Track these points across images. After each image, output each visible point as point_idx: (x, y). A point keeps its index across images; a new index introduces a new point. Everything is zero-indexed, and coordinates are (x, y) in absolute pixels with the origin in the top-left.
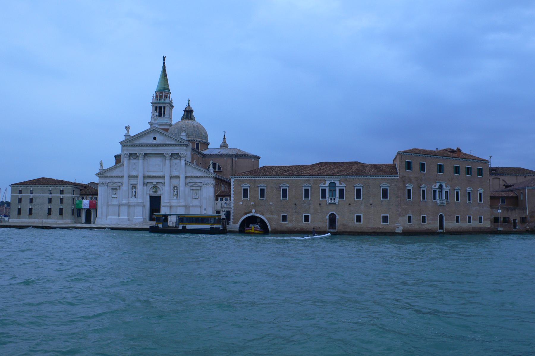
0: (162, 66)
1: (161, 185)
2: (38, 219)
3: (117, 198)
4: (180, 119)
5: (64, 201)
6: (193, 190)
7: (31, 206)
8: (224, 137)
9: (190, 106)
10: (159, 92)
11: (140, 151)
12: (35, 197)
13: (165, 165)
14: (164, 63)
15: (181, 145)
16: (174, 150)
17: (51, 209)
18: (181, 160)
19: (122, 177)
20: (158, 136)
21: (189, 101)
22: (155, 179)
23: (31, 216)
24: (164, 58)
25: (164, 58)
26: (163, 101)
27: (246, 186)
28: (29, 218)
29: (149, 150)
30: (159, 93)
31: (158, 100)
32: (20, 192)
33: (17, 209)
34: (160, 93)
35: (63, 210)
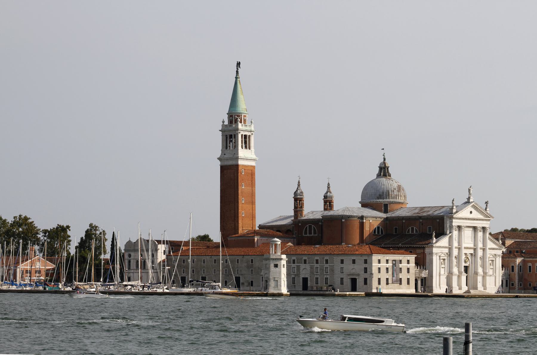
2: (393, 289)
3: (444, 268)
4: (375, 177)
5: (410, 270)
6: (491, 260)
8: (329, 184)
9: (386, 161)
11: (463, 224)
12: (390, 267)
14: (237, 72)
15: (488, 220)
16: (482, 224)
17: (401, 278)
20: (473, 210)
22: (468, 250)
23: (388, 285)
24: (239, 64)
25: (239, 64)
26: (248, 128)
28: (386, 289)
32: (379, 261)
34: (244, 116)
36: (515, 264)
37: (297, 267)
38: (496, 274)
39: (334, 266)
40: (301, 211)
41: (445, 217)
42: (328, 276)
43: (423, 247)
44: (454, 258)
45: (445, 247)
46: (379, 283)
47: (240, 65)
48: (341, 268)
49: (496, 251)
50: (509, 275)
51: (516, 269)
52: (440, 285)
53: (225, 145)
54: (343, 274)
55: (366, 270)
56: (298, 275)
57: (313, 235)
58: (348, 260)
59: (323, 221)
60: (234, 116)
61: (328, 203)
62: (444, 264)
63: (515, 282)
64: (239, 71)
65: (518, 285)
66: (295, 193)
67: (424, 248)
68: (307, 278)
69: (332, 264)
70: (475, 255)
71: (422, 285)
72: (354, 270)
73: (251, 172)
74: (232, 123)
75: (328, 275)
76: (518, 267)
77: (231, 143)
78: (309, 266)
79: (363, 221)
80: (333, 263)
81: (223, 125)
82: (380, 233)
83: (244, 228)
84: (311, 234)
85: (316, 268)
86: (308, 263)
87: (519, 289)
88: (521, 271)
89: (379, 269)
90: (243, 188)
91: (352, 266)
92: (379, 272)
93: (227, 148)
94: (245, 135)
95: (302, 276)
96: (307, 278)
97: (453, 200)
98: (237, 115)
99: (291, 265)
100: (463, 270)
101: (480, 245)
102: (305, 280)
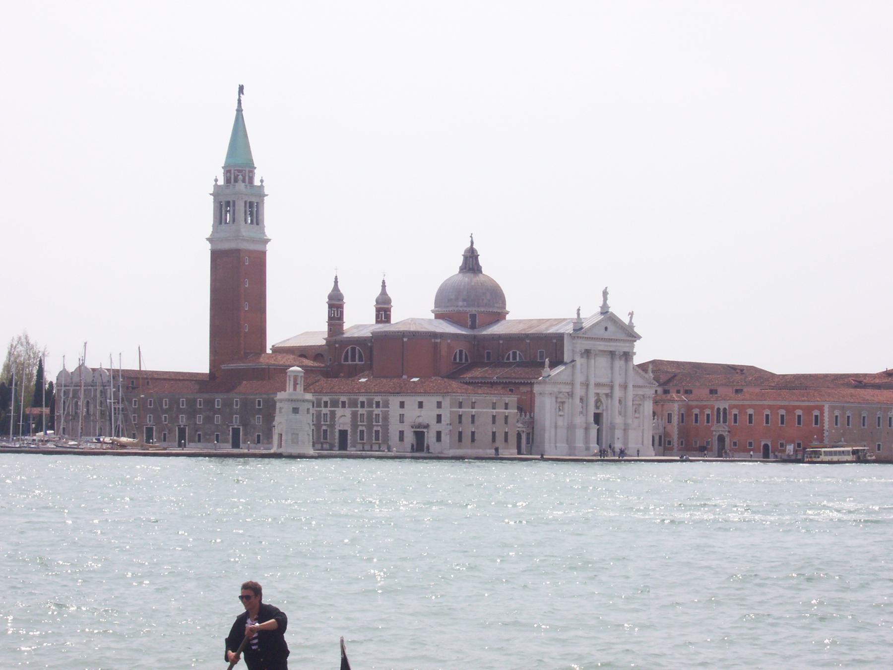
0: (236, 108)
1: (604, 396)
5: (510, 420)
6: (637, 404)
7: (473, 429)
8: (384, 282)
9: (474, 246)
10: (247, 169)
13: (612, 368)
18: (629, 362)
19: (572, 384)
21: (471, 237)
24: (241, 89)
25: (241, 89)
27: (837, 413)
29: (601, 346)
30: (247, 172)
31: (248, 187)
32: (460, 405)
33: (458, 433)
35: (509, 434)
36: (673, 411)
37: (330, 414)
38: (643, 426)
39: (388, 411)
40: (341, 325)
41: (566, 336)
42: (379, 428)
43: (531, 382)
44: (578, 401)
45: (565, 383)
46: (460, 440)
47: (244, 91)
48: (400, 415)
49: (645, 389)
50: (665, 428)
51: (675, 419)
52: (556, 442)
53: (218, 217)
54: (404, 424)
55: (439, 418)
56: (332, 426)
57: (357, 362)
58: (411, 401)
59: (373, 340)
60: (232, 172)
61: (383, 311)
62: (563, 410)
63: (673, 439)
64: (241, 99)
65: (678, 444)
66: (331, 297)
67: (532, 384)
68: (346, 431)
69: (386, 409)
70: (611, 397)
71: (528, 442)
72: (420, 418)
73: (258, 263)
74: (230, 183)
75: (380, 425)
76: (679, 415)
77: (228, 215)
78: (350, 412)
79: (436, 341)
80: (389, 407)
81: (216, 186)
82: (464, 361)
83: (248, 351)
84: (355, 361)
85: (361, 414)
86: (348, 407)
87: (679, 450)
88: (682, 422)
89: (460, 416)
90: (247, 286)
91: (418, 412)
92: (460, 422)
93: (221, 223)
94: (250, 202)
95: (338, 428)
96: (346, 431)
97: (579, 310)
98: (237, 170)
99: (321, 411)
100: (591, 419)
101: (618, 380)
102: (343, 433)
